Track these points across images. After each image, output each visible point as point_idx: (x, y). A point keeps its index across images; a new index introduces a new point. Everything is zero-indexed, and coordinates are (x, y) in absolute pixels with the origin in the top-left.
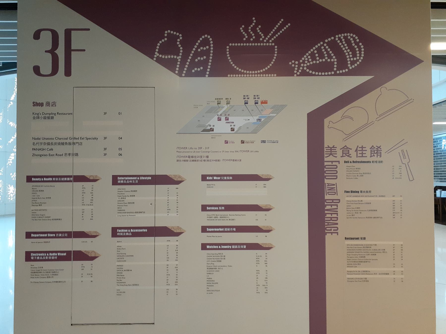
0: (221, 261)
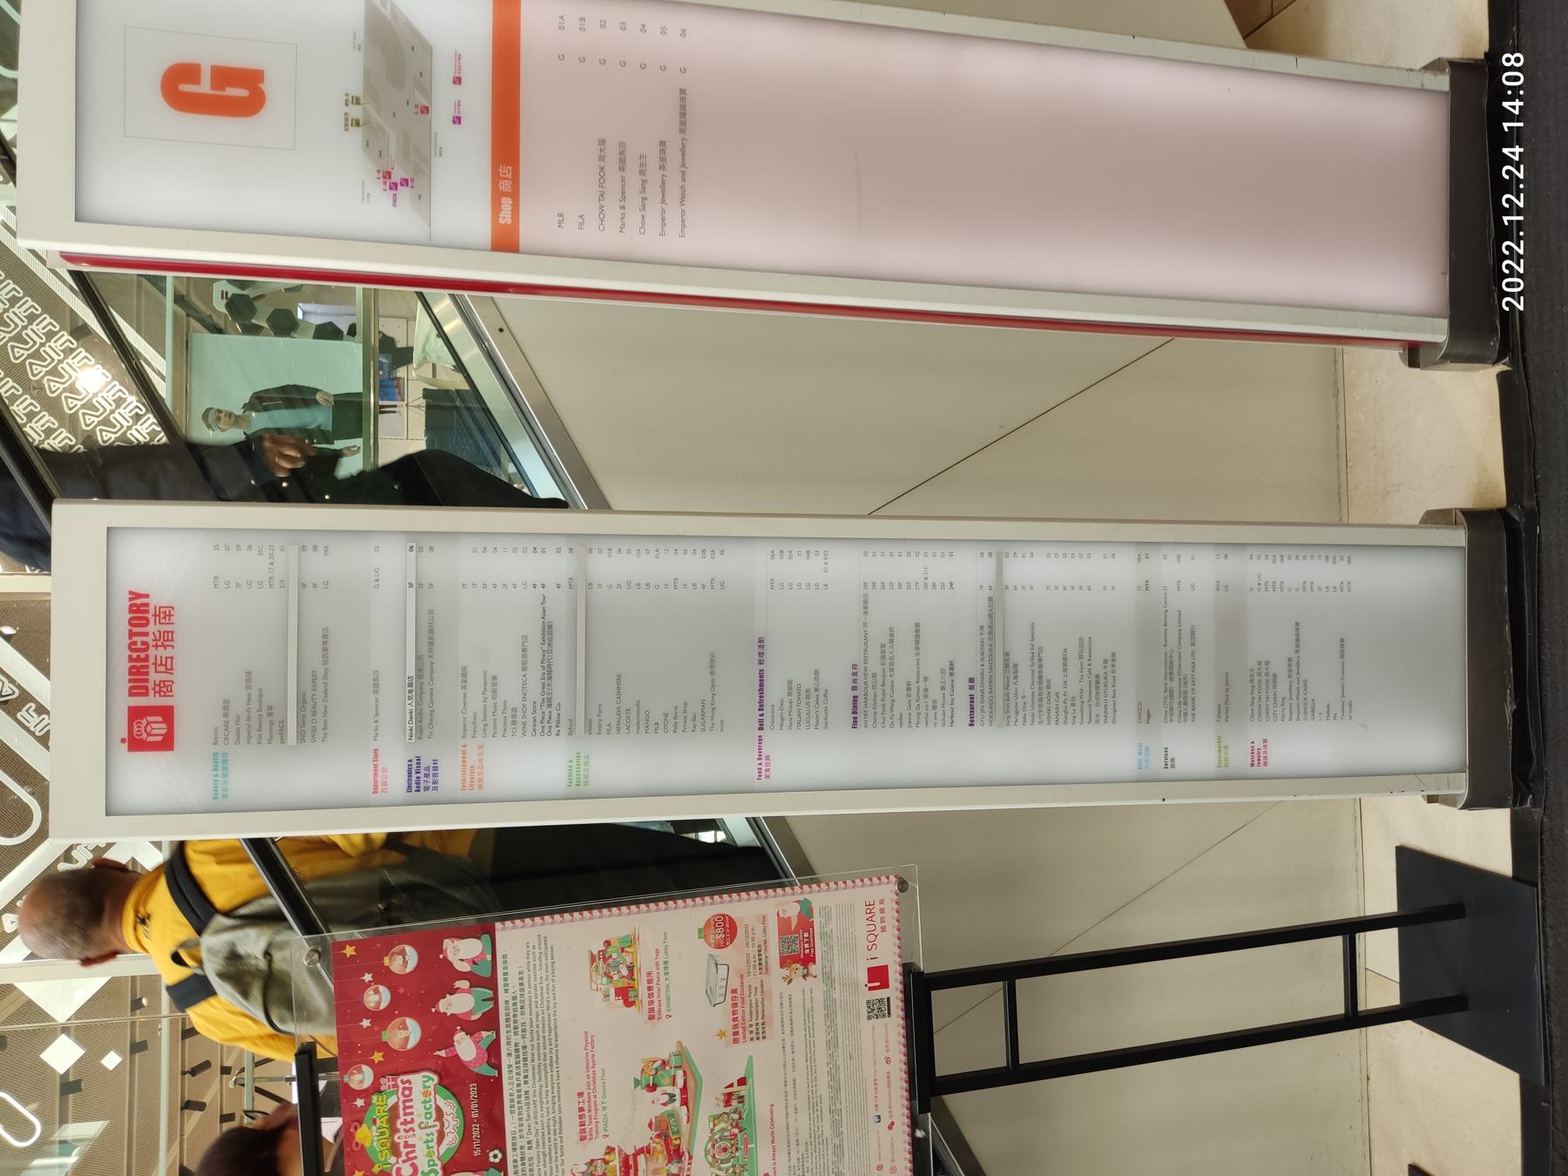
0: (1275, 676)
